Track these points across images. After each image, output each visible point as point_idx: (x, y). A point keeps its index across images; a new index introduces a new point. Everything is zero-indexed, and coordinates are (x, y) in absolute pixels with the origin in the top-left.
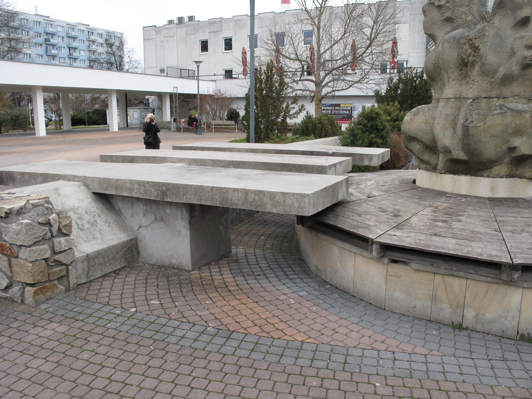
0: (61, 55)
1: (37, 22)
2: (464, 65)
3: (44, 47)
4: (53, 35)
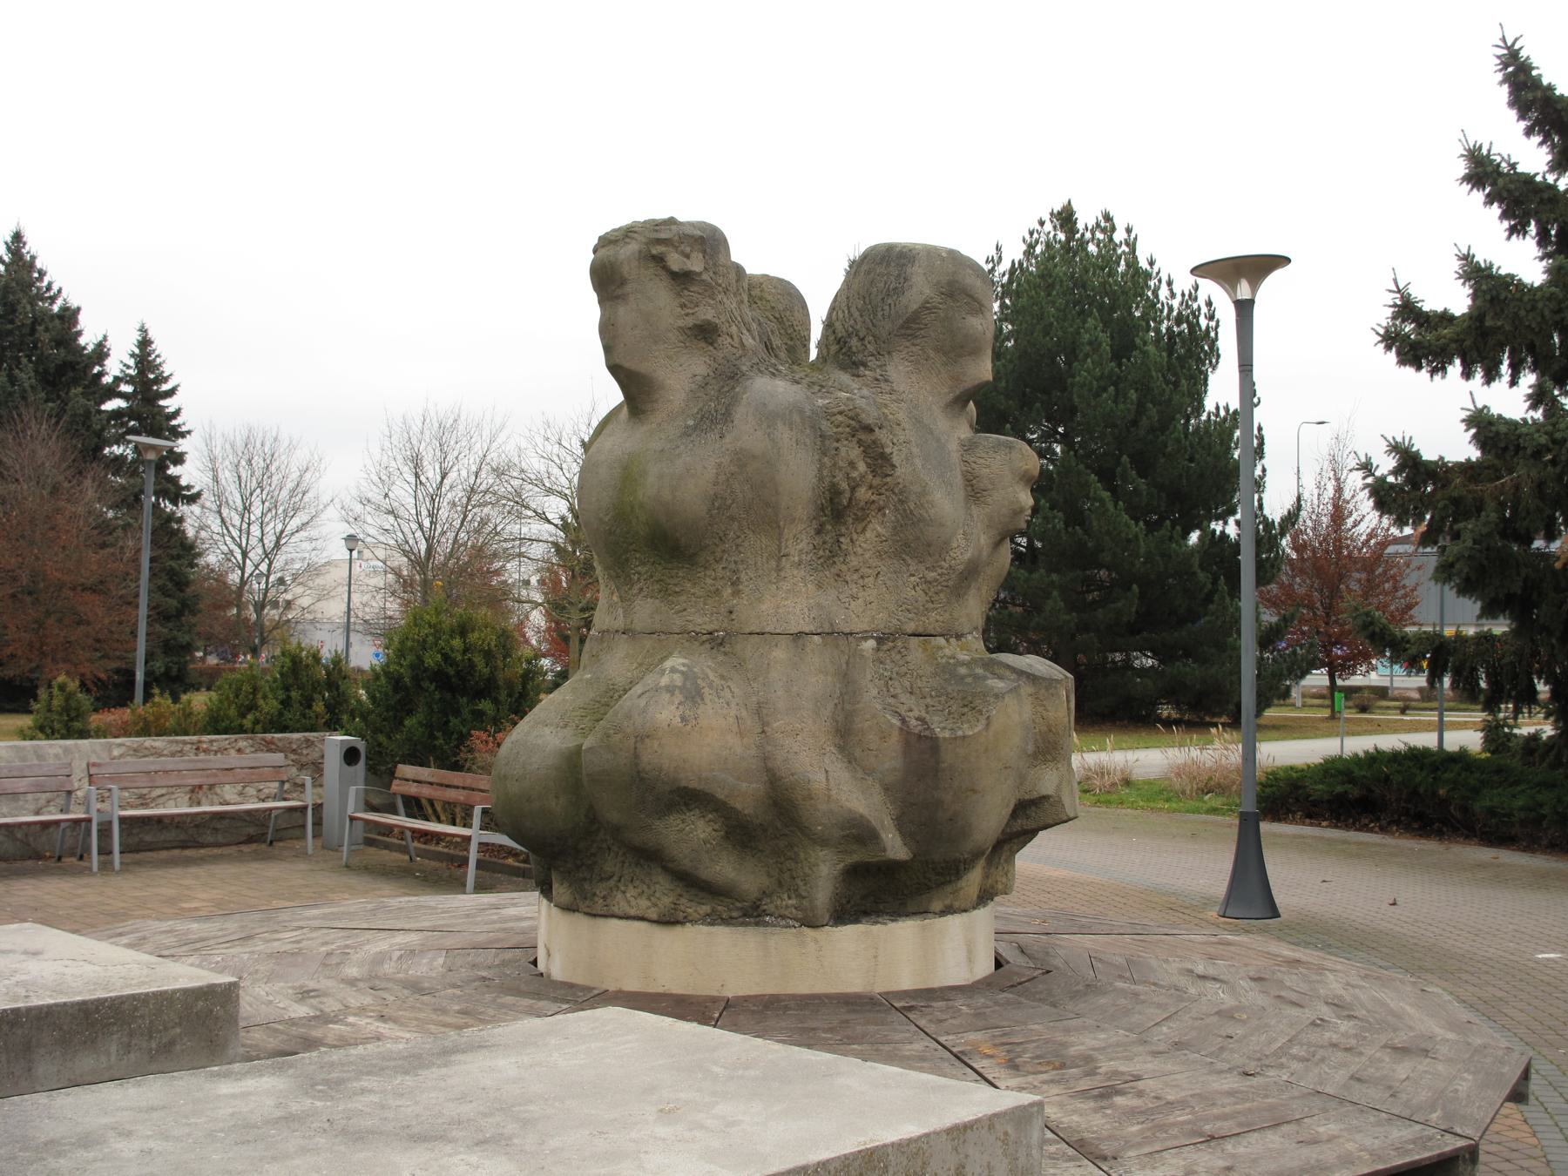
2: (835, 511)
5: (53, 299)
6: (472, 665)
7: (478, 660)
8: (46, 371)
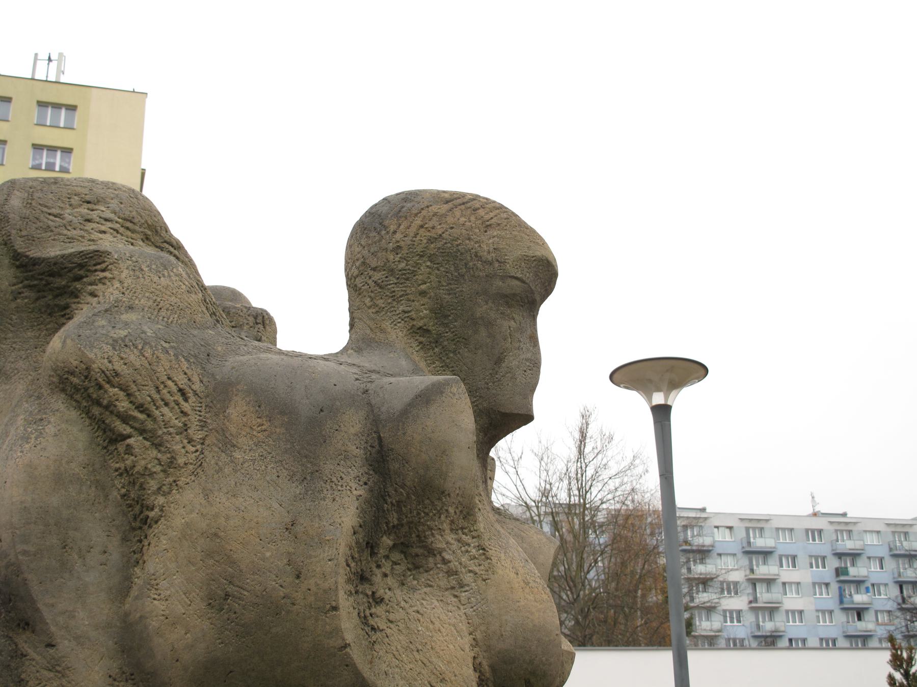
0: (878, 606)
1: (813, 531)
3: (834, 587)
4: (854, 556)
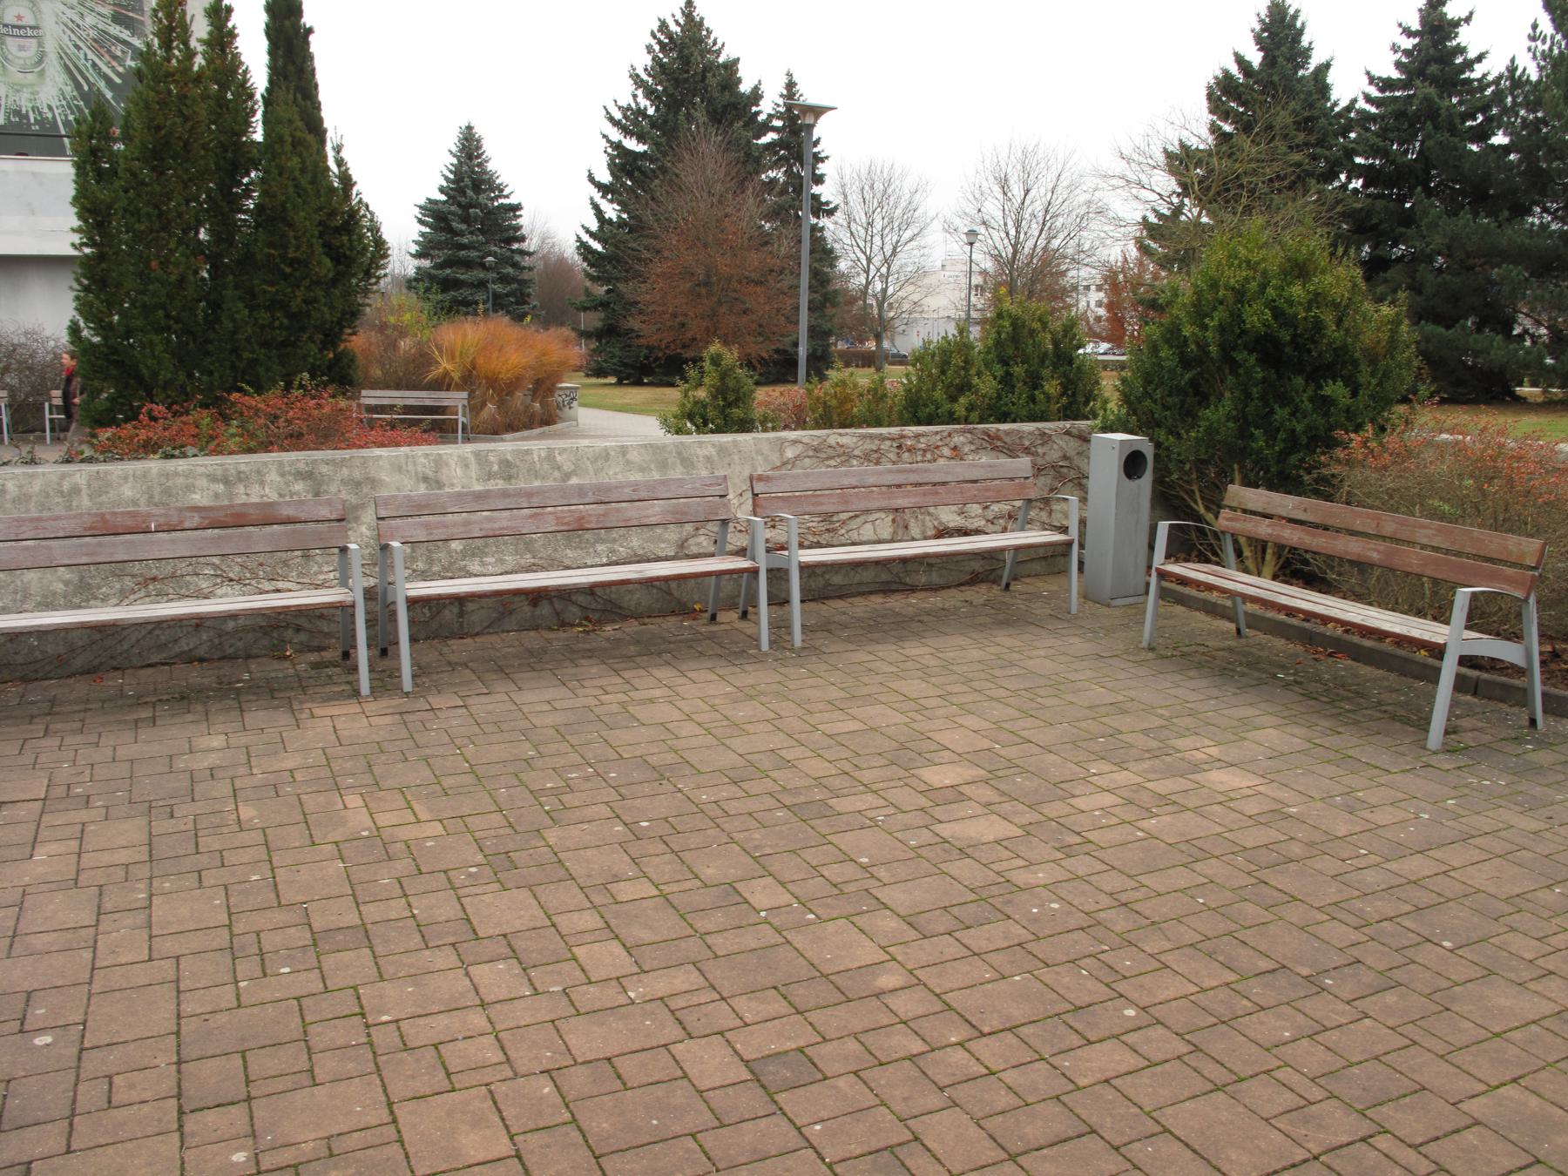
5: (718, 53)
6: (1318, 326)
7: (1328, 318)
8: (715, 111)
